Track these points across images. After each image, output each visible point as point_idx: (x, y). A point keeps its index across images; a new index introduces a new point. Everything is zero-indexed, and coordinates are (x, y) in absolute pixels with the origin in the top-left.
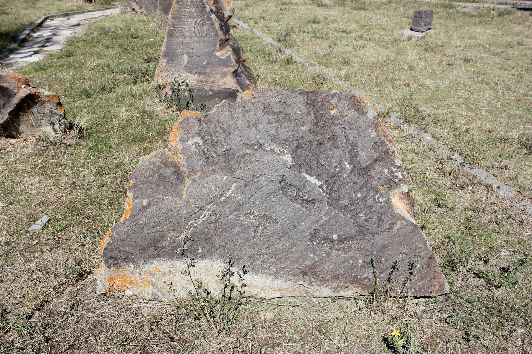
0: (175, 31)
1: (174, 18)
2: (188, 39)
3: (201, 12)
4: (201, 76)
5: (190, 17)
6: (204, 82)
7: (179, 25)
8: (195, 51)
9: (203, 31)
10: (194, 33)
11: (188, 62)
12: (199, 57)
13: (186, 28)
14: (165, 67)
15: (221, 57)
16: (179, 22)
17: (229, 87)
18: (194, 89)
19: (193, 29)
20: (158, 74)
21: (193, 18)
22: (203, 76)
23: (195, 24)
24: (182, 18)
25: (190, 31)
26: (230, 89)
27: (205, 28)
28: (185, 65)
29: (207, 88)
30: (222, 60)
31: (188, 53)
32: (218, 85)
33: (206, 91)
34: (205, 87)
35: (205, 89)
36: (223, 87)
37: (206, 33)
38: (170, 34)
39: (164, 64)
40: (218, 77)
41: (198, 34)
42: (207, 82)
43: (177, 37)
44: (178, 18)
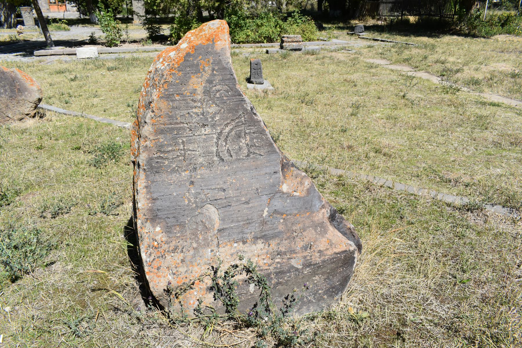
0: (167, 159)
1: (159, 132)
2: (202, 171)
3: (233, 110)
4: (273, 243)
5: (204, 126)
6: (285, 253)
7: (177, 144)
8: (231, 193)
9: (240, 149)
10: (218, 155)
11: (223, 220)
12: (247, 203)
13: (196, 151)
14: (167, 243)
15: (295, 194)
16: (175, 139)
17: (344, 248)
18: (269, 275)
19: (215, 149)
20: (156, 264)
21: (213, 126)
22: (277, 241)
23: (218, 138)
24: (184, 129)
25: (207, 153)
26: (346, 251)
27: (243, 142)
28: (217, 226)
29: (297, 263)
30: (299, 198)
31: (214, 201)
32: (320, 251)
33: (297, 269)
34: (293, 262)
35: (293, 267)
36: (330, 252)
37: (246, 151)
38: (152, 167)
39: (161, 237)
40: (310, 234)
41: (226, 157)
42: (293, 252)
43: (174, 171)
44: (173, 129)
